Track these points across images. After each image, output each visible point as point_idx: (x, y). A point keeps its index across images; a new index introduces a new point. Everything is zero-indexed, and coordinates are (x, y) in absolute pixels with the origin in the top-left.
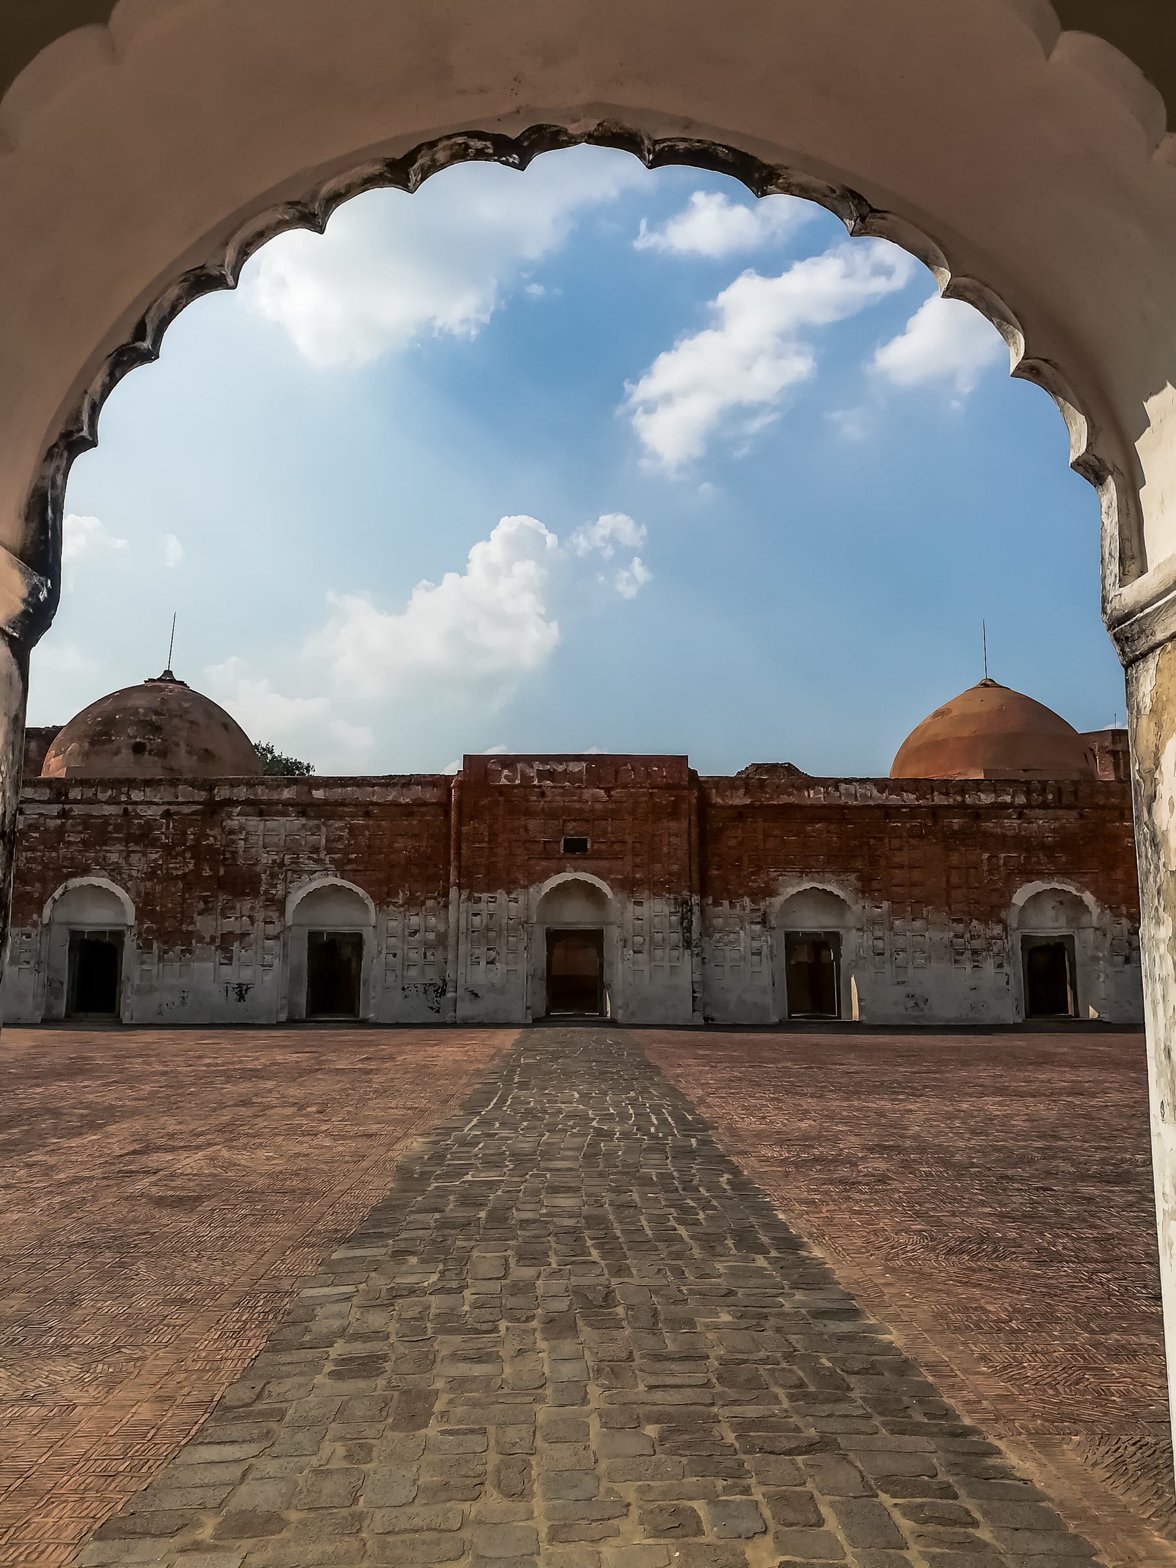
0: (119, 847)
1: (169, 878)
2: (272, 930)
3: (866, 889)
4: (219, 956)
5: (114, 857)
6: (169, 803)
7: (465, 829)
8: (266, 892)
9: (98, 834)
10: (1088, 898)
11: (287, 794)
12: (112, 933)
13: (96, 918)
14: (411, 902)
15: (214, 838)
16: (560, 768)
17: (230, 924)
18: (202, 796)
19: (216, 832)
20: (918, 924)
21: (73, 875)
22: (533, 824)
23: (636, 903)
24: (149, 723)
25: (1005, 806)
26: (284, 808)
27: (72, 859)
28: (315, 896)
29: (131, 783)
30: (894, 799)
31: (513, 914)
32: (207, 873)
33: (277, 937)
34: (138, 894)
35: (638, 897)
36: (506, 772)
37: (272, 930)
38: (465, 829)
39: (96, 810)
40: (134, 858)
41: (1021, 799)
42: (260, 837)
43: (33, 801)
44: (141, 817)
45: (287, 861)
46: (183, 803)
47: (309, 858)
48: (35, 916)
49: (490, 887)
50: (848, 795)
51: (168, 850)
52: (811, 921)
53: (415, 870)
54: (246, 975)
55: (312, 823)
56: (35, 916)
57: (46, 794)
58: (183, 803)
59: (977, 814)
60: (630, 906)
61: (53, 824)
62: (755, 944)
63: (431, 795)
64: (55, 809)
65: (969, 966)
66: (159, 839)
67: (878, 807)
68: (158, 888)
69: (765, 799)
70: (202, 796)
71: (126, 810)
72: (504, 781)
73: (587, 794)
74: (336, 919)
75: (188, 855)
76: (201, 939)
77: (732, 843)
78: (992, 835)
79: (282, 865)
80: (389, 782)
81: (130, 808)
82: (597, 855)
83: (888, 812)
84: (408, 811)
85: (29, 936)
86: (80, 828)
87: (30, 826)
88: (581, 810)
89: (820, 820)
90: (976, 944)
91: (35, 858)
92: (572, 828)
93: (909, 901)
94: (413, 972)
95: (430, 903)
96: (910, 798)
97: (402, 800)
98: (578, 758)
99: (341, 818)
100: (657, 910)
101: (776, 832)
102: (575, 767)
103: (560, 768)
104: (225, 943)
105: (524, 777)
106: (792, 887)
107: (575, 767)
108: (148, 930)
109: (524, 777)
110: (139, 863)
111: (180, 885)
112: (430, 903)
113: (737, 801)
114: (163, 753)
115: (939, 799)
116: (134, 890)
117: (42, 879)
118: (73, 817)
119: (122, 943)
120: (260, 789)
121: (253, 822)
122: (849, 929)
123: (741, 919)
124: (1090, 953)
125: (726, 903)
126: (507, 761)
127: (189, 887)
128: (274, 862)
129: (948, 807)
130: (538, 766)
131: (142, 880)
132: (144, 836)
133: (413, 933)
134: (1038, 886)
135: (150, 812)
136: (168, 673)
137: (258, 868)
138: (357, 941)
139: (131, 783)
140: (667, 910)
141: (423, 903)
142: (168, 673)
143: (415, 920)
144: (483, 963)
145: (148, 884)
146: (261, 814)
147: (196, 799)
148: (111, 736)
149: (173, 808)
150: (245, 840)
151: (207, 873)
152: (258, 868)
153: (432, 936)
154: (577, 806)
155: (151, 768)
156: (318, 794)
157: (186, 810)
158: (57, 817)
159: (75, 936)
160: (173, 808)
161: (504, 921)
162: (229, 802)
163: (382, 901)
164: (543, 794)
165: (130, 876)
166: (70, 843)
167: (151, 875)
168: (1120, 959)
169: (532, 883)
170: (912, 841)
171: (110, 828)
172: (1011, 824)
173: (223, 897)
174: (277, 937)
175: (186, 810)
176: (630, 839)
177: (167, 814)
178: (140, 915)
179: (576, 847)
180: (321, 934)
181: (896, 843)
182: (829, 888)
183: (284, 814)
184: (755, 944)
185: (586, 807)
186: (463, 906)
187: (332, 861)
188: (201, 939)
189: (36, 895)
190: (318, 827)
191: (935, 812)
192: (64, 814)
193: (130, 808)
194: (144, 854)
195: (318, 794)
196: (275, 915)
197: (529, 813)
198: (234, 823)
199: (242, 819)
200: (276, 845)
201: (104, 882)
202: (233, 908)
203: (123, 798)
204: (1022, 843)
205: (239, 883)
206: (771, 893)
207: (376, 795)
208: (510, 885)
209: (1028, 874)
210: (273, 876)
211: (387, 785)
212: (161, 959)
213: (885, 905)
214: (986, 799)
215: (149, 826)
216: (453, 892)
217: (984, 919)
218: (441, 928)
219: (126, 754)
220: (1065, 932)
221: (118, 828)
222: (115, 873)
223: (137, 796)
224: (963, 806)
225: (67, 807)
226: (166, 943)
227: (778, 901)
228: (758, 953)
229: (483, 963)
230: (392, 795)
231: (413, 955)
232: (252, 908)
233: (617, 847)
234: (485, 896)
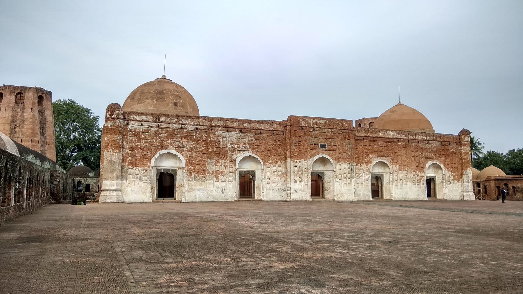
0: (178, 140)
1: (197, 151)
2: (231, 170)
3: (392, 162)
4: (215, 179)
5: (177, 143)
6: (197, 125)
7: (292, 140)
8: (230, 157)
9: (171, 134)
10: (442, 166)
11: (236, 124)
12: (173, 170)
13: (167, 164)
14: (275, 162)
15: (212, 138)
16: (319, 121)
17: (217, 168)
18: (208, 123)
19: (213, 136)
20: (405, 172)
21: (162, 149)
22: (311, 139)
23: (340, 164)
24: (176, 96)
25: (424, 140)
26: (234, 129)
27: (162, 143)
28: (244, 159)
29: (183, 117)
30: (400, 137)
31: (306, 167)
32: (210, 150)
33: (233, 172)
34: (187, 157)
35: (340, 162)
36: (303, 122)
37: (231, 170)
38: (292, 140)
39: (170, 126)
40: (185, 144)
41: (428, 138)
42: (228, 139)
43: (147, 121)
44: (186, 129)
45: (236, 147)
46: (202, 125)
47: (243, 146)
48: (149, 163)
49: (300, 157)
50: (389, 134)
51: (196, 141)
52: (377, 171)
53: (275, 152)
54: (223, 185)
55: (243, 135)
56: (149, 163)
57: (151, 119)
58: (202, 125)
59: (418, 142)
60: (338, 165)
61: (154, 130)
62: (367, 177)
63: (279, 128)
64: (155, 124)
65: (416, 184)
66: (192, 138)
67: (396, 139)
68: (194, 154)
69: (369, 134)
70: (208, 123)
71: (182, 127)
72: (303, 125)
73: (326, 130)
74: (248, 167)
75: (203, 143)
76: (209, 173)
77: (361, 147)
78: (422, 148)
79: (234, 148)
80: (266, 122)
81: (183, 126)
82: (329, 150)
83: (398, 140)
84: (273, 132)
85: (146, 171)
86: (164, 132)
87: (145, 130)
88: (324, 135)
89: (382, 141)
90: (418, 178)
91: (148, 142)
92: (322, 141)
93: (404, 166)
94: (274, 185)
95: (279, 163)
96: (403, 136)
97: (270, 129)
98: (323, 119)
99: (252, 133)
100: (344, 166)
101: (372, 144)
102: (322, 121)
103: (319, 121)
104: (217, 174)
105: (309, 123)
106: (376, 160)
107: (322, 121)
108: (191, 169)
109: (309, 123)
110: (187, 145)
111: (201, 154)
112: (279, 163)
113: (362, 135)
114: (183, 106)
115: (410, 137)
116: (185, 155)
117: (151, 150)
118: (161, 128)
119: (176, 173)
120: (227, 122)
121: (225, 133)
122: (387, 173)
123: (363, 170)
124: (441, 181)
125: (359, 165)
126: (304, 118)
127: (204, 154)
128: (232, 147)
129: (412, 139)
130: (312, 120)
131: (188, 151)
132: (188, 137)
133: (275, 172)
134: (431, 162)
135: (190, 127)
136: (164, 76)
137: (227, 149)
138: (253, 174)
139: (183, 117)
140: (348, 167)
141: (277, 163)
142: (164, 76)
143: (275, 168)
144: (298, 182)
145: (190, 153)
146: (228, 131)
147: (206, 124)
148: (164, 99)
149: (198, 127)
150: (222, 139)
151: (210, 150)
152: (227, 149)
153: (280, 173)
154: (323, 134)
155: (180, 111)
156: (246, 125)
157: (203, 128)
158: (156, 127)
159: (158, 170)
160: (198, 127)
161: (304, 169)
162: (217, 126)
163: (265, 162)
164: (314, 129)
165: (183, 150)
166: (161, 137)
167: (191, 150)
168: (449, 183)
169: (311, 157)
170: (404, 149)
171: (175, 132)
172: (425, 145)
173: (215, 158)
174: (233, 172)
175: (203, 128)
176: (337, 145)
177: (197, 129)
178: (188, 163)
179: (323, 146)
180: (242, 171)
181: (400, 149)
182: (384, 161)
183: (234, 131)
184: (367, 177)
185: (325, 134)
186: (292, 164)
187: (250, 147)
188: (209, 173)
189: (149, 156)
190: (245, 136)
191: (409, 140)
192: (158, 127)
193: (183, 126)
194: (188, 142)
195: (246, 125)
196: (233, 165)
197: (310, 136)
198: (218, 133)
199: (221, 132)
200: (233, 141)
201: (174, 152)
202: (219, 162)
203: (180, 122)
204: (427, 150)
205: (221, 154)
206: (370, 162)
207: (263, 127)
208: (306, 158)
209: (429, 159)
210: (231, 152)
211: (266, 123)
212: (195, 180)
213: (398, 166)
214: (420, 137)
215: (190, 132)
216: (289, 160)
217: (420, 171)
218: (283, 170)
219: (171, 105)
220: (434, 175)
221: (178, 133)
222: (178, 148)
223: (185, 122)
224: (415, 139)
225: (160, 124)
226: (196, 174)
227: (372, 165)
228: (368, 180)
229: (298, 182)
230: (268, 127)
231: (274, 179)
232: (225, 162)
233: (334, 147)
234: (298, 161)
